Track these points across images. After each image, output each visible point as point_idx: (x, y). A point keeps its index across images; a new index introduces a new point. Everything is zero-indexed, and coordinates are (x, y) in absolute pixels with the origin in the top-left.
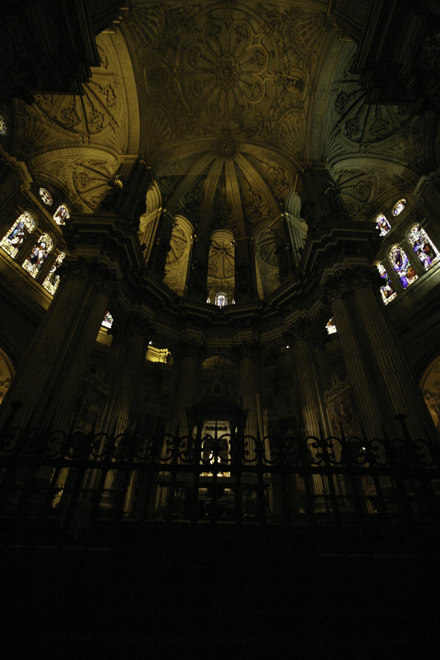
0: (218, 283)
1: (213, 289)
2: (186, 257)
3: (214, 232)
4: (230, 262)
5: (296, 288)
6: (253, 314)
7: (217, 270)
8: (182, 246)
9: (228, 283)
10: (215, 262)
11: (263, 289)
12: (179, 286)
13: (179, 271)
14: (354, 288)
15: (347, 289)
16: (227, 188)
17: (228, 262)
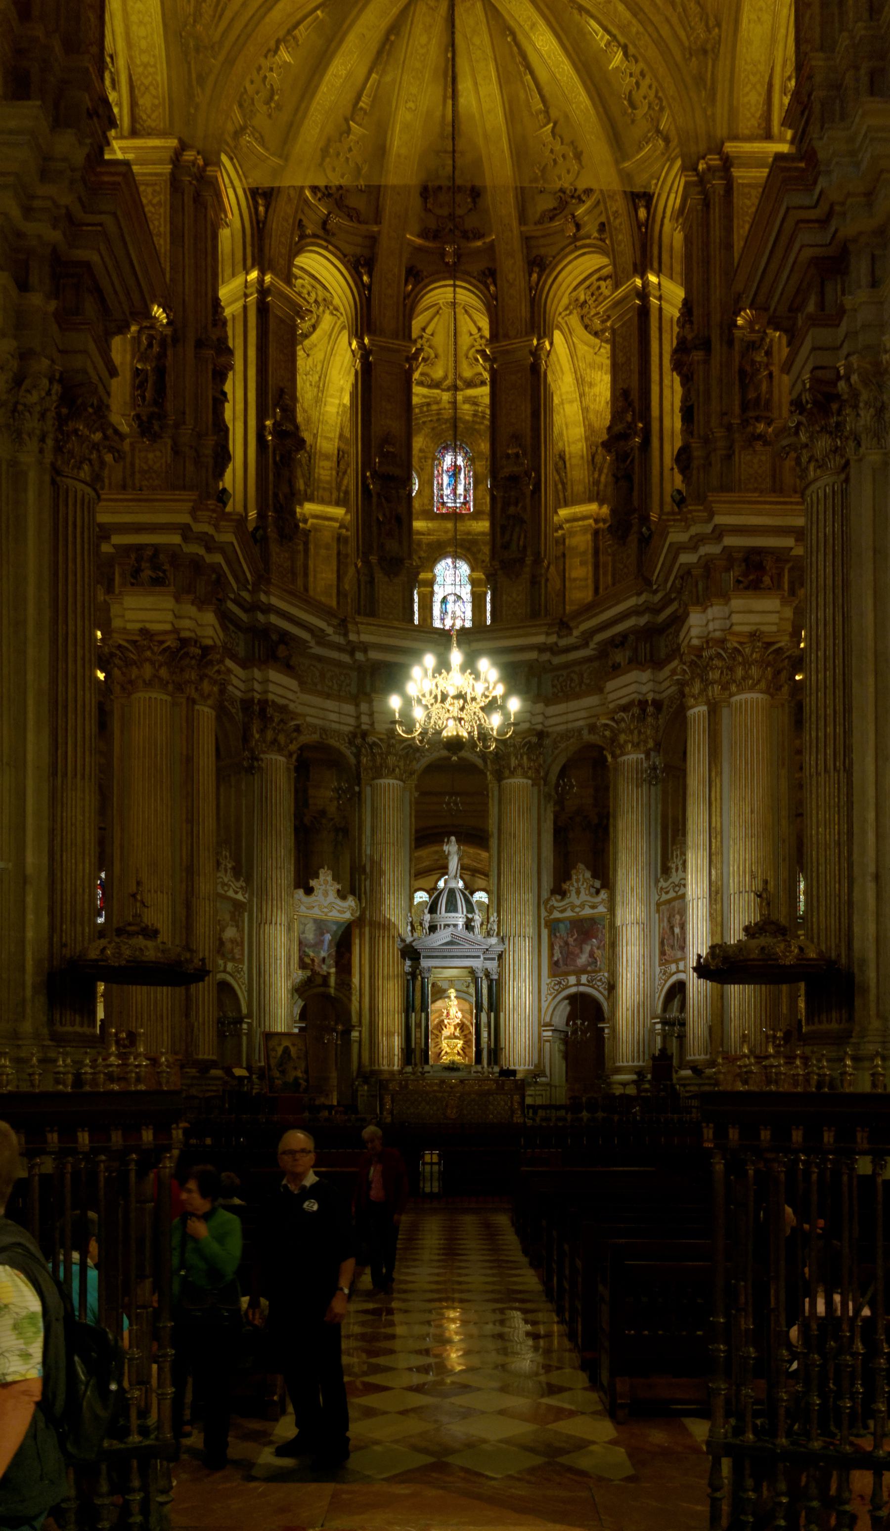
0: (442, 406)
1: (426, 430)
2: (330, 336)
3: (424, 291)
4: (479, 329)
5: (635, 612)
6: (533, 655)
7: (436, 357)
8: (313, 295)
9: (475, 404)
10: (429, 330)
11: (587, 439)
12: (315, 436)
13: (310, 377)
14: (734, 688)
15: (717, 688)
16: (462, 101)
17: (474, 331)
